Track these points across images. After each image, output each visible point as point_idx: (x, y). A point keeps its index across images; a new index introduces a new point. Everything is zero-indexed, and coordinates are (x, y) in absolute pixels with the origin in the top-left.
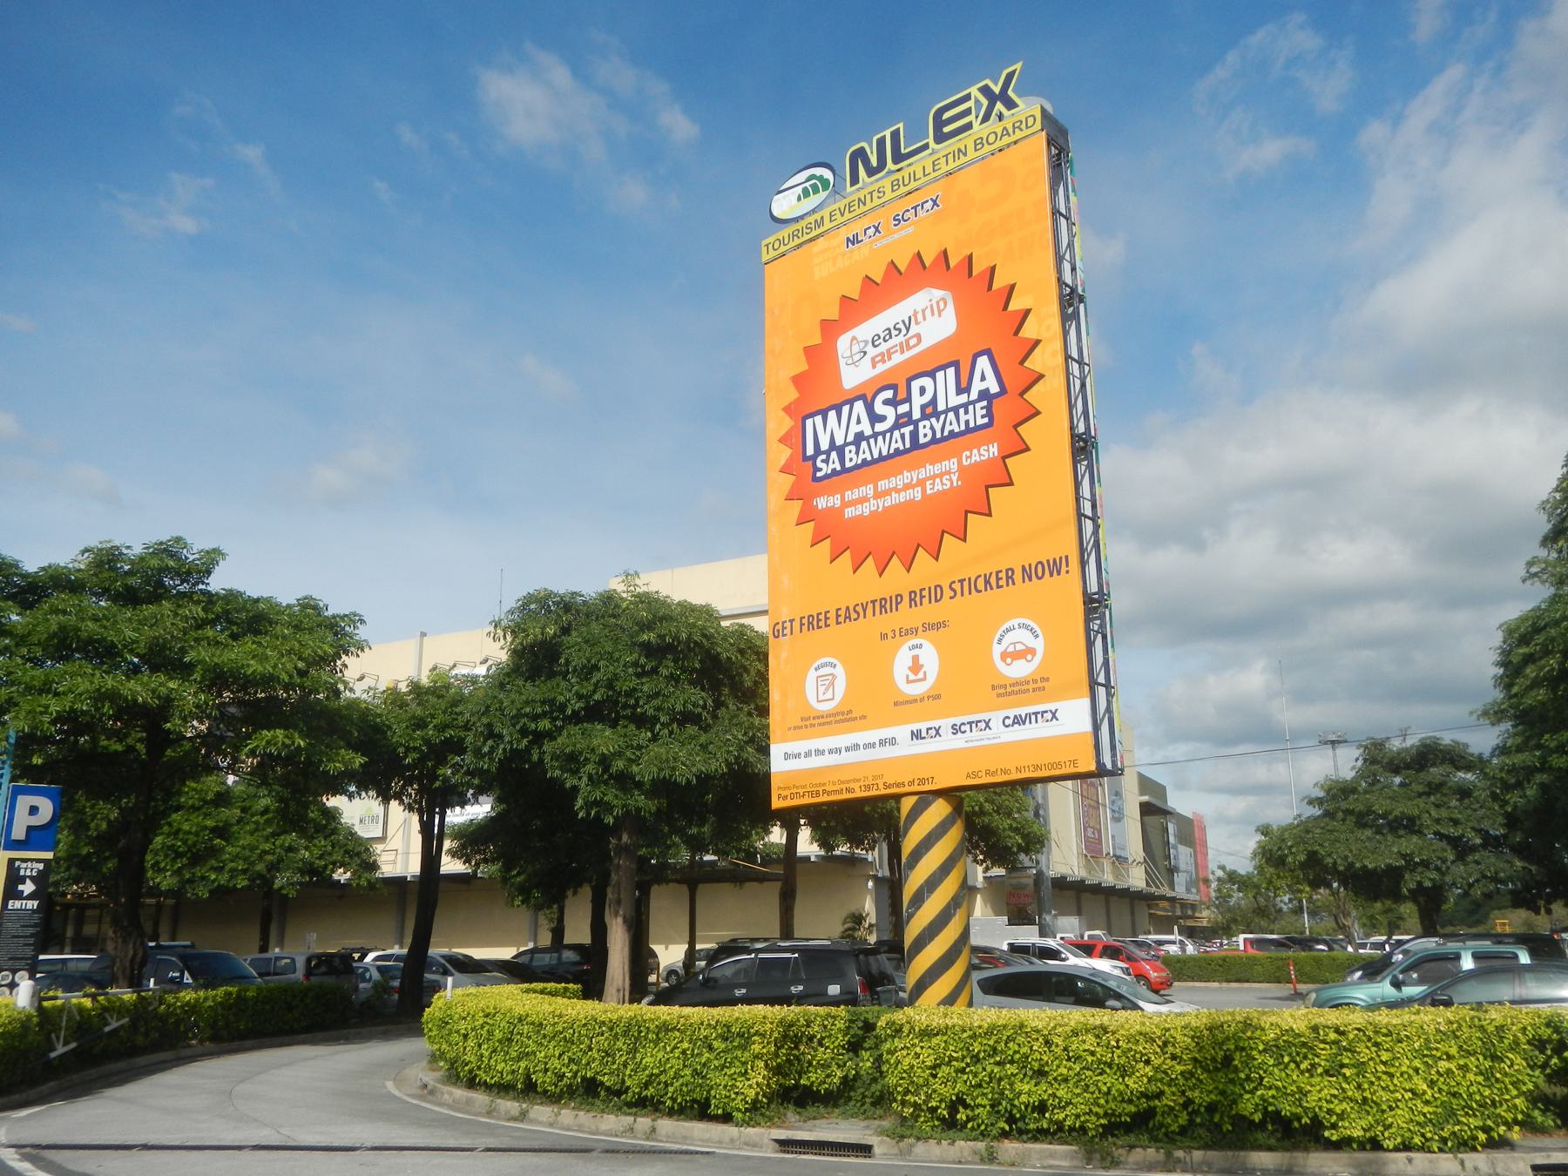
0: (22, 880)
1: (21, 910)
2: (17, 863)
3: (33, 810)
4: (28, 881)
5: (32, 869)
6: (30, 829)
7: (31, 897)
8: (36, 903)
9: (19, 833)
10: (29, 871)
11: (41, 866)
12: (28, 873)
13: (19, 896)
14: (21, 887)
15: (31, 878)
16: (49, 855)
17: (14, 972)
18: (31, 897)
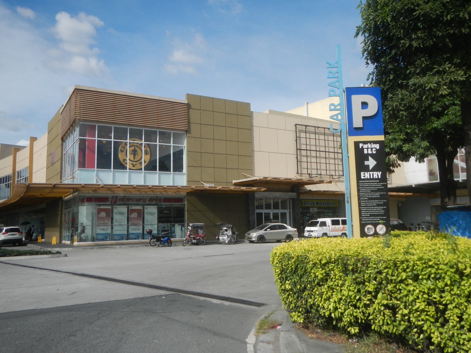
0: (366, 157)
1: (370, 179)
2: (361, 145)
3: (365, 105)
4: (370, 158)
5: (372, 149)
6: (364, 118)
7: (375, 169)
8: (380, 174)
9: (358, 123)
10: (370, 150)
11: (377, 146)
12: (370, 152)
13: (366, 169)
14: (366, 163)
15: (372, 156)
16: (381, 138)
17: (375, 225)
18: (375, 169)
